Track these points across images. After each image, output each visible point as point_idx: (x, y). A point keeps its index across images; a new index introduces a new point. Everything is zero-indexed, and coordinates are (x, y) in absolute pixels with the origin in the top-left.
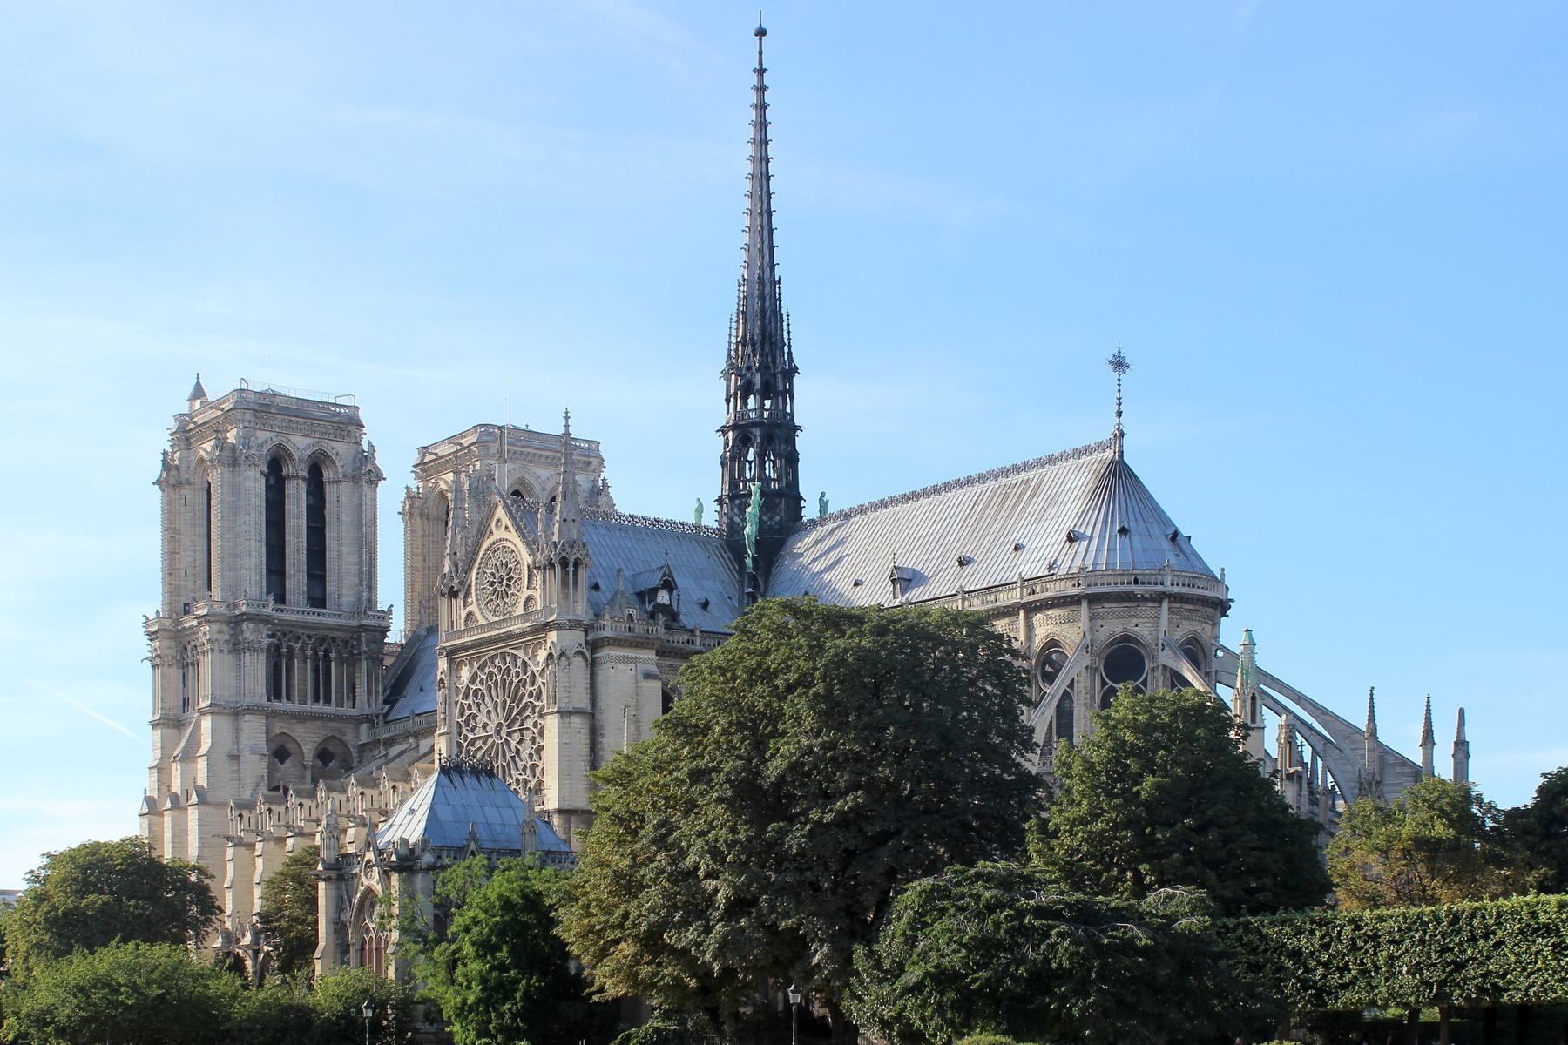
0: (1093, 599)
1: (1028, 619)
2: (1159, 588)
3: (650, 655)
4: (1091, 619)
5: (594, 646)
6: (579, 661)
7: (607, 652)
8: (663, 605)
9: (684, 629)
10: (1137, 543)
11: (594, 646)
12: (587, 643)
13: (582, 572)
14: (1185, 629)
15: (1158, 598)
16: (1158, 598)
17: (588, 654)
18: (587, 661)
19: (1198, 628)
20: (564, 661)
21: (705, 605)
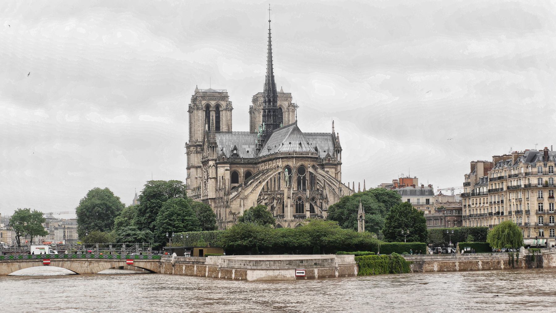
0: (282, 158)
1: (276, 161)
2: (293, 156)
3: (229, 165)
4: (282, 162)
5: (217, 164)
6: (214, 167)
7: (219, 165)
8: (235, 153)
9: (240, 158)
10: (291, 146)
11: (217, 164)
12: (216, 163)
13: (214, 149)
14: (299, 164)
15: (293, 157)
16: (293, 157)
17: (215, 165)
18: (215, 167)
19: (303, 163)
20: (211, 168)
21: (248, 152)
